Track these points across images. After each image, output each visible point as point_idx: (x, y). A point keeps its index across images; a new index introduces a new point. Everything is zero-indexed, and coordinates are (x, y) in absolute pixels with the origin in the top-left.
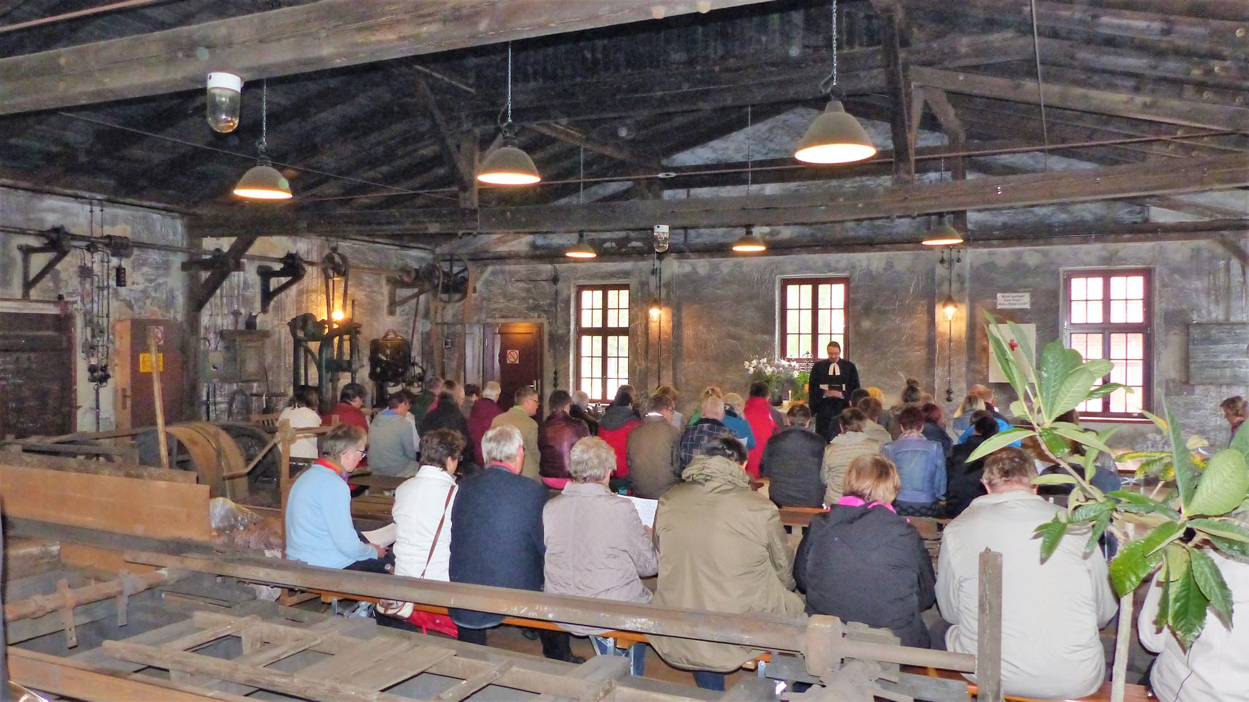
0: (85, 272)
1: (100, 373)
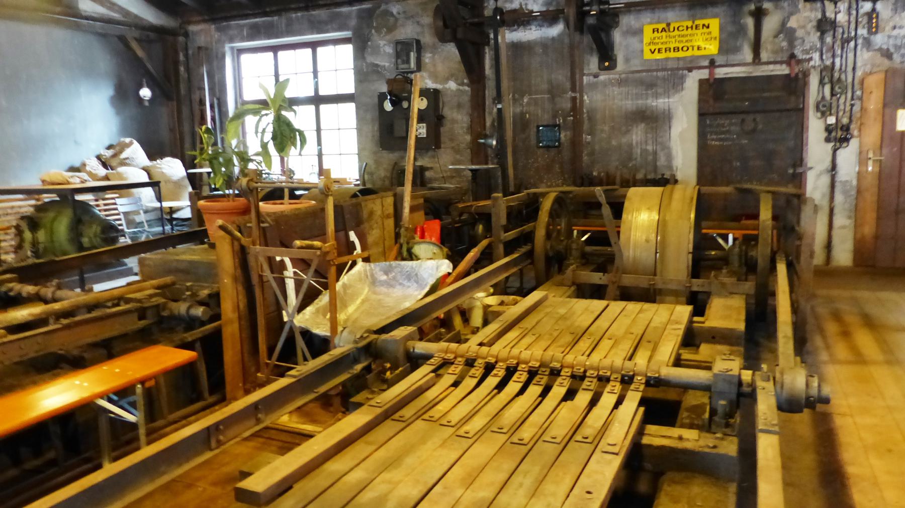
0: (825, 25)
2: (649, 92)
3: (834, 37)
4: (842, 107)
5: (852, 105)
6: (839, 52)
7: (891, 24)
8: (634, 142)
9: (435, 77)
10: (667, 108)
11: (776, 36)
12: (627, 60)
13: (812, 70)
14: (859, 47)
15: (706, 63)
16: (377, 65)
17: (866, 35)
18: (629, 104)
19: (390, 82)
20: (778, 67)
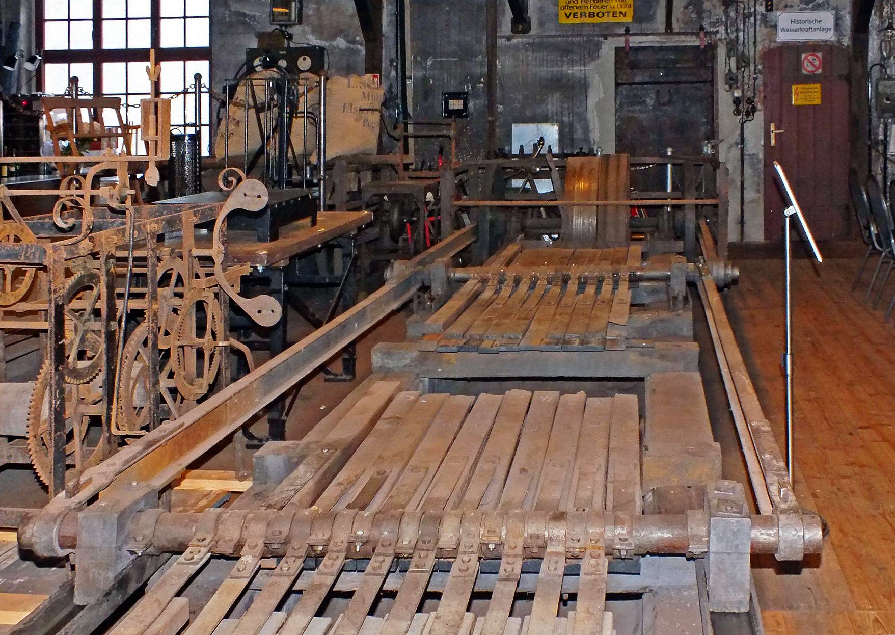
1: (746, 105)
2: (565, 59)
3: (737, 12)
4: (746, 80)
5: (755, 79)
6: (742, 27)
7: (783, 3)
8: (550, 112)
9: (318, 31)
10: (582, 76)
11: (686, 7)
12: (541, 24)
13: (719, 43)
14: (758, 22)
15: (622, 31)
16: (244, 15)
17: (764, 12)
18: (545, 71)
19: (261, 36)
20: (688, 38)
